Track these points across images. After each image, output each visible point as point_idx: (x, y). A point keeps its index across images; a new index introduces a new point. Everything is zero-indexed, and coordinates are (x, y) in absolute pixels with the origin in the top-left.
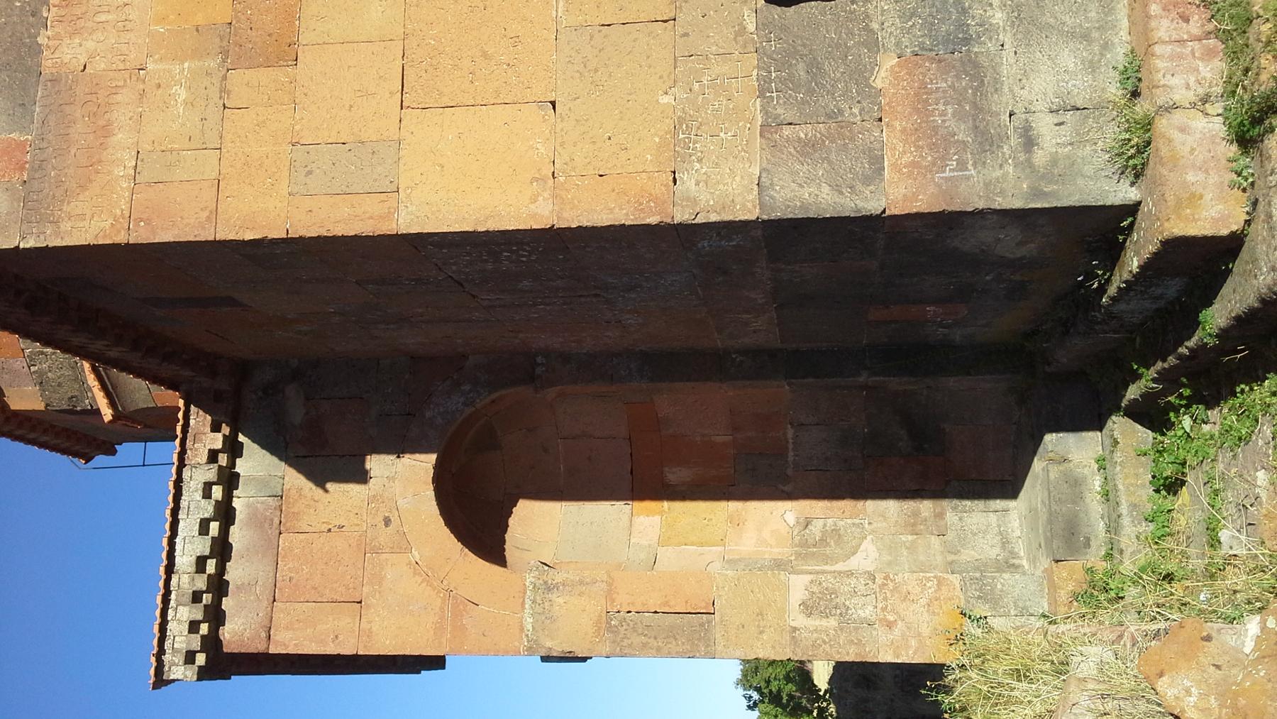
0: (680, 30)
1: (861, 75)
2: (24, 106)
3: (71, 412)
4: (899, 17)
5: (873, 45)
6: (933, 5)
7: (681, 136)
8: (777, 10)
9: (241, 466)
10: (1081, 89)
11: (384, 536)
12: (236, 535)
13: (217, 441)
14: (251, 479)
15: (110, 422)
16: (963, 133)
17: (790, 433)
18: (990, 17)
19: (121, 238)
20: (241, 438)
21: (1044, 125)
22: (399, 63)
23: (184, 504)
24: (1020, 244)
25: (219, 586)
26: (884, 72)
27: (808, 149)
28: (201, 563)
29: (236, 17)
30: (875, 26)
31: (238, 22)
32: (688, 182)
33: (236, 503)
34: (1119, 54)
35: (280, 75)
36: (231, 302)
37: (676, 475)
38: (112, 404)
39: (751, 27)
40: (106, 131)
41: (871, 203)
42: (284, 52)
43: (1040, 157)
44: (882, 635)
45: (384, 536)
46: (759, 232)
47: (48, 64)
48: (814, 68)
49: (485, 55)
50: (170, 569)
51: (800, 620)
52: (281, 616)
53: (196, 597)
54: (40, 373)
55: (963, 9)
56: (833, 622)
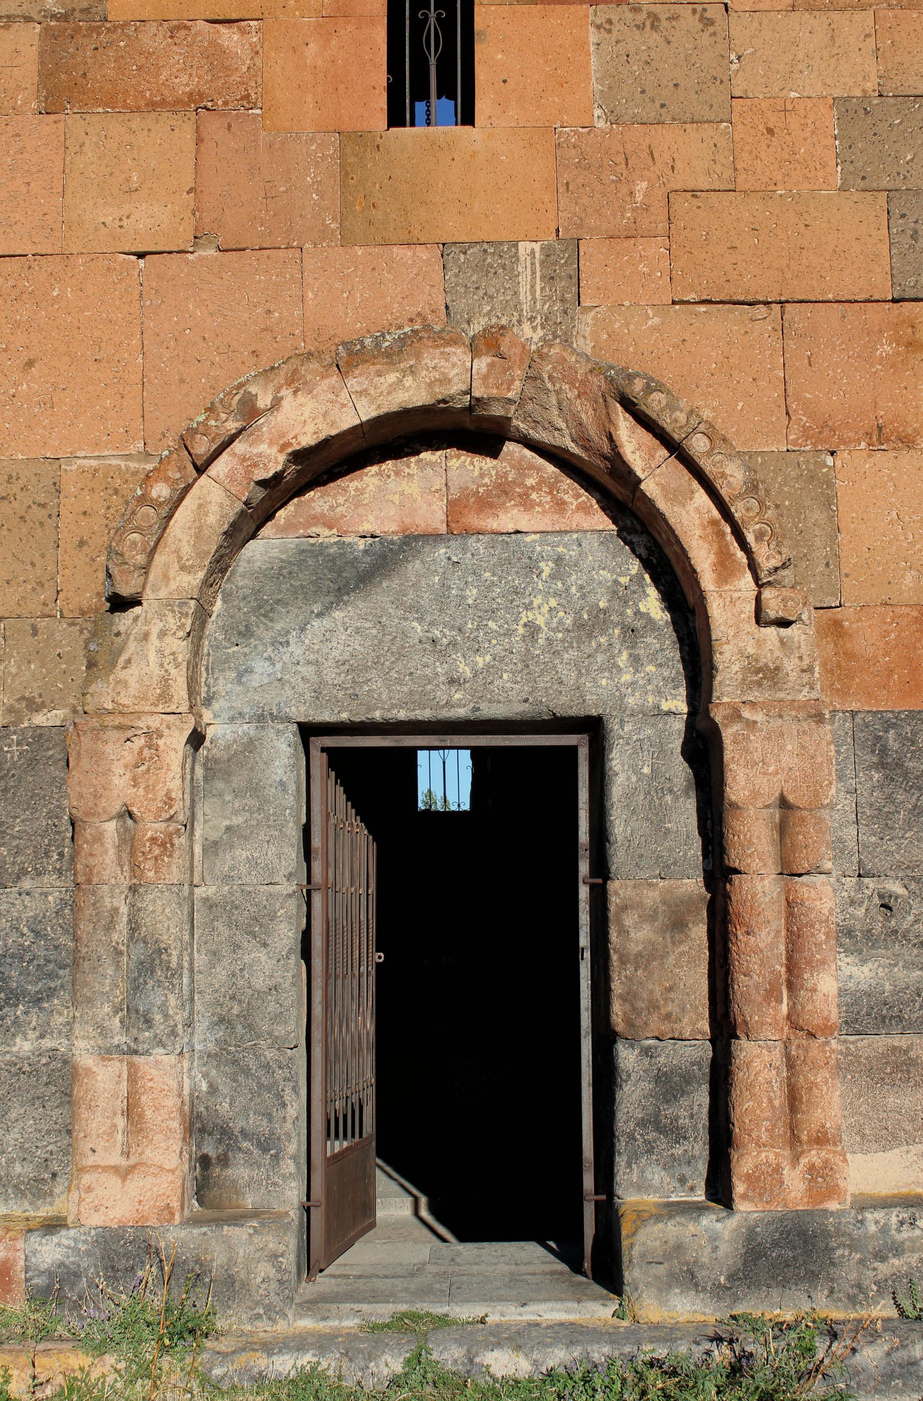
0: (42, 624)
4: (35, 917)
6: (49, 961)
18: (25, 1035)
22: (29, 249)
29: (115, 27)
30: (27, 884)
31: (108, 30)
39: (40, 719)
49: (30, 364)
55: (39, 1000)
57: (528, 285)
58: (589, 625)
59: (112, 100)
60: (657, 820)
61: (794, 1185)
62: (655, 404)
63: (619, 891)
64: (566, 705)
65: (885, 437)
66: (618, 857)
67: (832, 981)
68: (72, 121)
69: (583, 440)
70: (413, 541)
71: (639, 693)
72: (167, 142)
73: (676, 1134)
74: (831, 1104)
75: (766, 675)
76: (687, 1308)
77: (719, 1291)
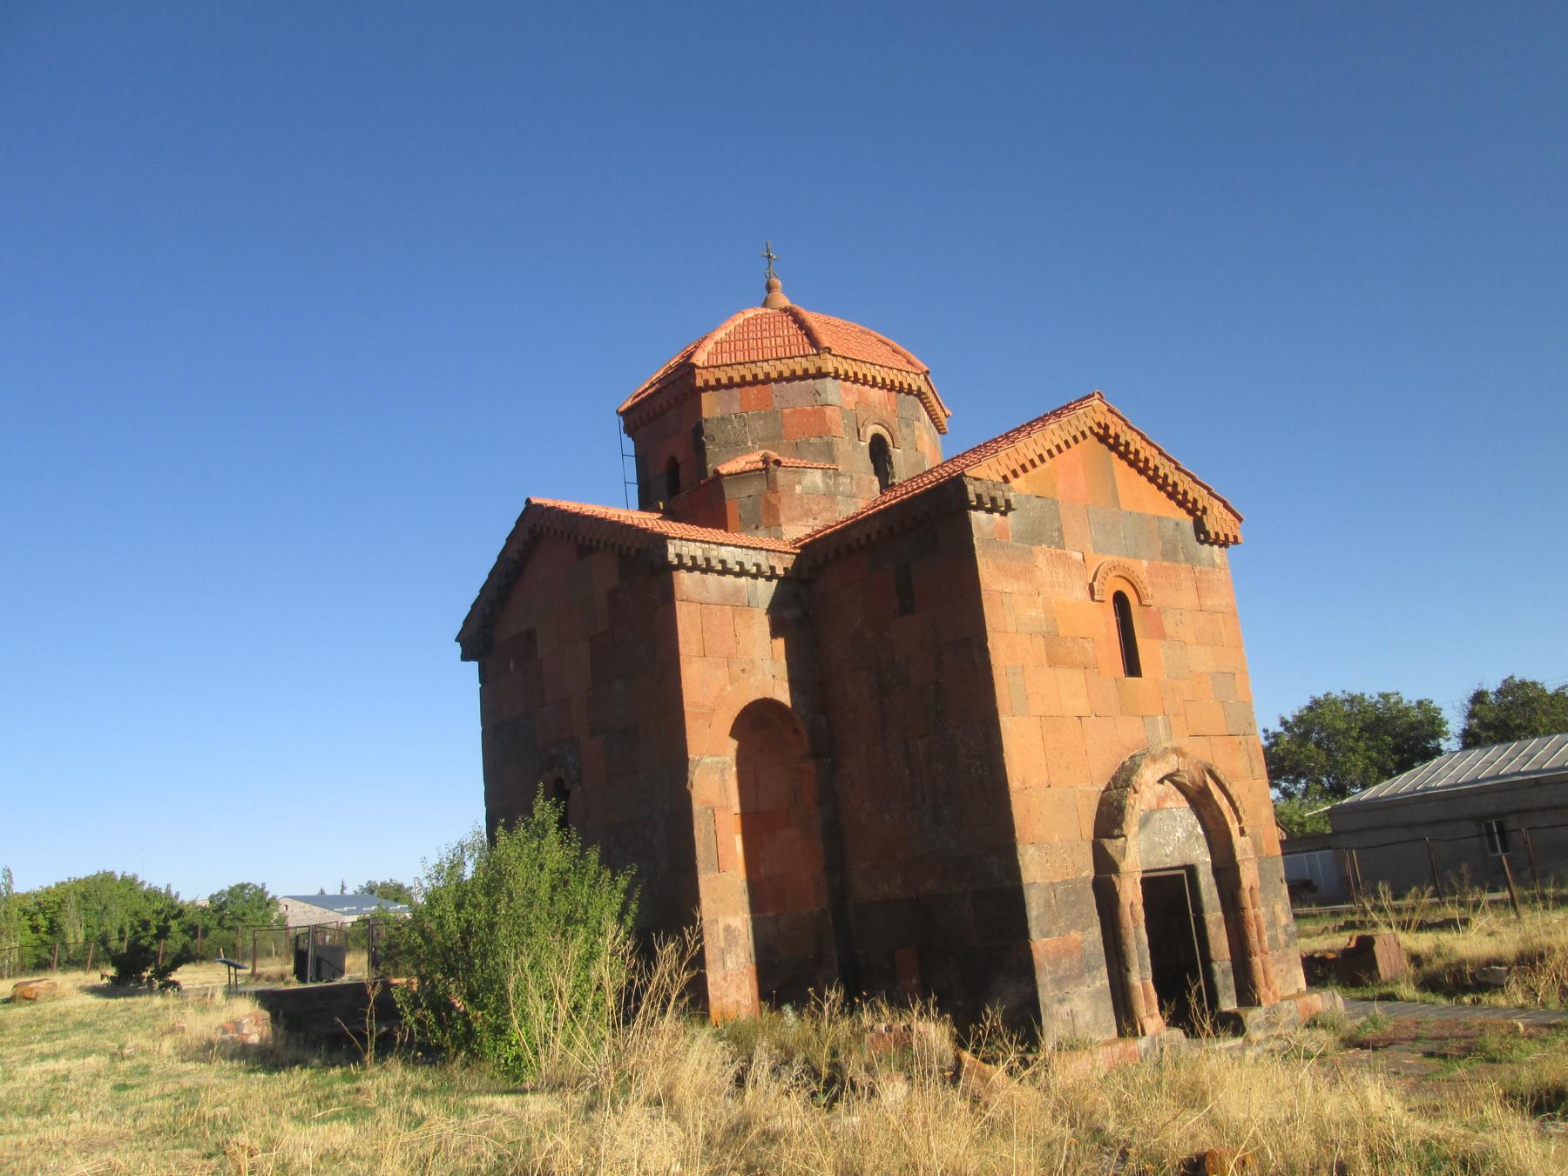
1: (1073, 925)
2: (1020, 537)
3: (698, 430)
5: (1084, 929)
9: (761, 581)
10: (1080, 1022)
11: (736, 669)
12: (729, 579)
13: (780, 572)
14: (755, 587)
15: (716, 472)
16: (1060, 972)
17: (771, 914)
19: (983, 587)
20: (775, 582)
21: (1066, 1008)
23: (751, 552)
25: (708, 569)
26: (1075, 935)
27: (1048, 903)
28: (723, 562)
33: (744, 579)
35: (1044, 660)
38: (730, 475)
39: (1084, 874)
40: (1017, 579)
41: (1034, 934)
42: (1053, 661)
43: (1056, 1006)
44: (719, 975)
45: (736, 669)
47: (1036, 549)
51: (721, 925)
52: (695, 607)
53: (708, 560)
57: (1161, 730)
58: (1188, 838)
60: (1210, 893)
62: (1218, 773)
67: (1265, 938)
69: (1193, 782)
70: (1152, 811)
71: (1202, 857)
72: (1078, 676)
73: (1228, 988)
74: (1273, 971)
75: (1245, 851)
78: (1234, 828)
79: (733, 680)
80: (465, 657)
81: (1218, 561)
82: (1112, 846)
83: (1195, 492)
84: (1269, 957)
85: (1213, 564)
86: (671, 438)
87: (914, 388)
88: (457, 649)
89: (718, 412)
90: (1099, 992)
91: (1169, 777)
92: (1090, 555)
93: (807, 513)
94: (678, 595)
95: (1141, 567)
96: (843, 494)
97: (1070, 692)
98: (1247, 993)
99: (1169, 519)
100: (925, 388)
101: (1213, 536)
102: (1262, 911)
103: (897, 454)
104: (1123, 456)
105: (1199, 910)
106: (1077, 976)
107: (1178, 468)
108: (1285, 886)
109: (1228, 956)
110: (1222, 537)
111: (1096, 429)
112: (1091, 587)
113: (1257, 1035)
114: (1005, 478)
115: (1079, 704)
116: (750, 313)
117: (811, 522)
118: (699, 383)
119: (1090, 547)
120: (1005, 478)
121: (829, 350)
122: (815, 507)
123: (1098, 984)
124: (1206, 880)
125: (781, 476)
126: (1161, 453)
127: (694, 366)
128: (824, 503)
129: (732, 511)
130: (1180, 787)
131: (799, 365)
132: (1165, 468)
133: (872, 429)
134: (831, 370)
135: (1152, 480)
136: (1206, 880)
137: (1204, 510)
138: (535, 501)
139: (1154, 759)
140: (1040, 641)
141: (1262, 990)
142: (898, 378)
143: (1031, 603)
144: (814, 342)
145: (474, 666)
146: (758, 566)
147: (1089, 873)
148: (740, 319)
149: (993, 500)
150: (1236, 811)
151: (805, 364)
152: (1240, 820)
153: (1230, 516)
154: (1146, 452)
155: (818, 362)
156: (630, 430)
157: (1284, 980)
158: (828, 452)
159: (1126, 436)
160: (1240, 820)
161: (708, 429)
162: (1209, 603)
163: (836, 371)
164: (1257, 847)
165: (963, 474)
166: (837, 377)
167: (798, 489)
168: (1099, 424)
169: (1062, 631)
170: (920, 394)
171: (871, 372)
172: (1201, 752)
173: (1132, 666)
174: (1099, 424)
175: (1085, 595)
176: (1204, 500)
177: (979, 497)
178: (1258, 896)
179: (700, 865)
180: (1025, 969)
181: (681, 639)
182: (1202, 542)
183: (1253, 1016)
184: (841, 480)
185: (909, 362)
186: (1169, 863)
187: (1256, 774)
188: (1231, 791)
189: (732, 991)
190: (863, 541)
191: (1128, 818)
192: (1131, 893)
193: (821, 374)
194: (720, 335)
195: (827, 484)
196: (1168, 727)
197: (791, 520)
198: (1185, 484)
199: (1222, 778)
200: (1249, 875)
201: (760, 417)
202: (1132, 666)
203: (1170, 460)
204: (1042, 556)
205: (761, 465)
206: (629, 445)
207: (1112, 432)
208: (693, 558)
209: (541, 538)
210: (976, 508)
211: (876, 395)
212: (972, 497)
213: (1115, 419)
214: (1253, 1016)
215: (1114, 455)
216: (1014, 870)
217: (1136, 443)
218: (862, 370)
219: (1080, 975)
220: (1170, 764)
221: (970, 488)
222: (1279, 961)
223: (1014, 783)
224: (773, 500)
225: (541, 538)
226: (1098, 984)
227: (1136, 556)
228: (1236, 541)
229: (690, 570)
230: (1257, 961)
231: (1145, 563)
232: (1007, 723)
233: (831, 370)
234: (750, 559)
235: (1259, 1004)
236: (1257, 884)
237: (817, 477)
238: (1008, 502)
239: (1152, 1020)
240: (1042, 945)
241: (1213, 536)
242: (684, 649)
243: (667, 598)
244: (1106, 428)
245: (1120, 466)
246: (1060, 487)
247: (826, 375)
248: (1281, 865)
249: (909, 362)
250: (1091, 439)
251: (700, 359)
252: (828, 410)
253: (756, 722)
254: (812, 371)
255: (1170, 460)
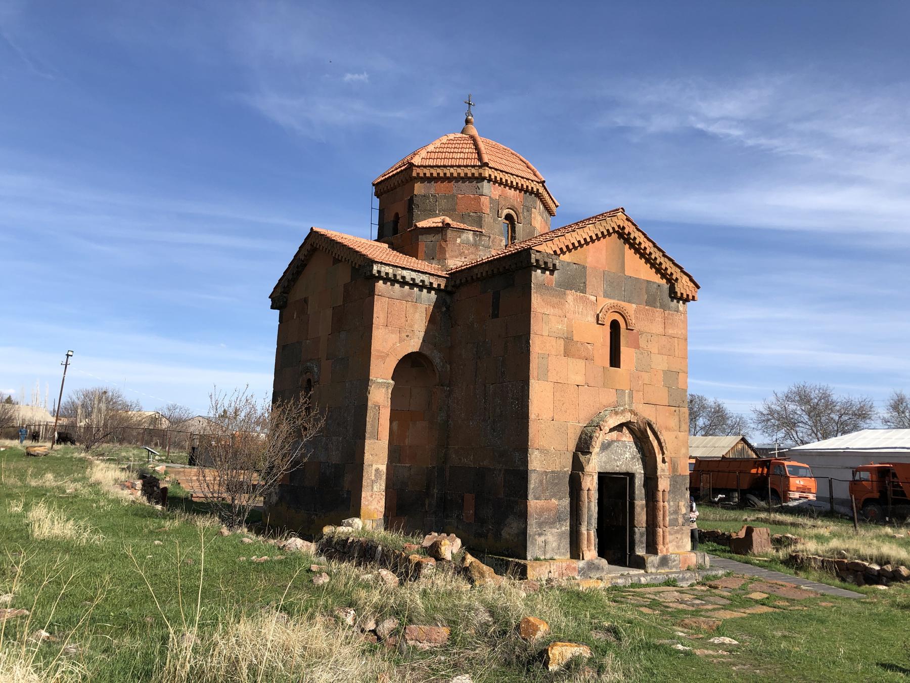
3: (411, 201)
5: (560, 499)
7: (544, 451)
8: (568, 476)
21: (543, 538)
24: (509, 534)
26: (554, 501)
27: (541, 482)
28: (403, 278)
32: (536, 453)
34: (555, 557)
35: (562, 352)
36: (495, 315)
37: (395, 424)
38: (423, 228)
40: (554, 307)
41: (530, 497)
42: (567, 354)
44: (369, 494)
45: (404, 335)
46: (522, 468)
47: (568, 292)
48: (557, 484)
50: (403, 268)
53: (395, 276)
54: (429, 198)
56: (373, 478)
57: (627, 399)
58: (633, 458)
59: (573, 356)
61: (665, 553)
62: (654, 426)
63: (636, 502)
64: (630, 471)
65: (668, 429)
66: (636, 497)
67: (667, 519)
68: (570, 360)
71: (638, 469)
72: (581, 363)
73: (642, 543)
74: (669, 538)
75: (663, 470)
76: (654, 570)
77: (657, 568)
78: (659, 458)
79: (401, 340)
80: (272, 308)
81: (681, 308)
82: (582, 458)
83: (672, 269)
84: (667, 530)
85: (677, 311)
86: (399, 204)
87: (535, 190)
88: (270, 302)
89: (423, 192)
90: (563, 533)
91: (627, 425)
92: (601, 299)
93: (461, 254)
94: (376, 293)
95: (631, 308)
96: (483, 246)
97: (575, 371)
98: (652, 548)
99: (654, 283)
100: (541, 190)
101: (679, 295)
102: (666, 503)
103: (519, 227)
104: (632, 246)
105: (632, 498)
106: (552, 523)
107: (664, 256)
108: (688, 492)
109: (644, 525)
110: (685, 296)
111: (617, 229)
112: (598, 315)
113: (651, 570)
114: (555, 252)
115: (580, 379)
116: (451, 136)
117: (463, 259)
118: (414, 174)
119: (601, 294)
120: (555, 252)
121: (486, 165)
122: (466, 252)
123: (563, 529)
124: (639, 481)
125: (449, 233)
126: (655, 246)
127: (411, 165)
128: (472, 249)
129: (422, 248)
130: (632, 431)
131: (469, 172)
132: (656, 254)
133: (506, 212)
134: (487, 175)
135: (648, 261)
136: (639, 481)
137: (677, 279)
138: (315, 229)
139: (616, 413)
140: (562, 342)
141: (660, 547)
142: (526, 183)
143: (561, 324)
144: (480, 158)
145: (277, 312)
146: (423, 281)
147: (568, 469)
148: (444, 139)
149: (546, 263)
150: (661, 448)
151: (473, 170)
152: (663, 453)
153: (692, 285)
154: (646, 244)
155: (481, 171)
156: (378, 195)
157: (678, 542)
158: (479, 221)
159: (635, 234)
160: (663, 453)
161: (415, 200)
162: (670, 332)
163: (490, 175)
164: (674, 468)
165: (531, 248)
166: (490, 180)
167: (459, 240)
168: (619, 226)
169: (575, 339)
170: (538, 195)
171: (510, 179)
172: (648, 413)
173: (615, 360)
174: (619, 226)
175: (594, 320)
176: (677, 274)
177: (537, 261)
178: (667, 497)
179: (367, 435)
180: (523, 515)
181: (375, 315)
182: (672, 298)
183: (652, 560)
184: (483, 238)
185: (535, 175)
186: (617, 470)
187: (682, 429)
188: (661, 437)
189: (375, 503)
190: (479, 276)
191: (593, 443)
192: (590, 483)
193: (481, 179)
194: (431, 148)
195: (475, 239)
196: (631, 397)
197: (452, 257)
198: (666, 264)
199: (656, 429)
200: (663, 484)
201: (445, 197)
202: (615, 360)
203: (659, 250)
204: (571, 296)
205: (440, 225)
206: (376, 202)
207: (626, 231)
208: (387, 274)
209: (316, 248)
210: (538, 267)
211: (512, 193)
212: (533, 261)
213: (630, 224)
214: (652, 560)
215: (627, 246)
216: (525, 462)
217: (640, 239)
218: (505, 177)
219: (554, 523)
220: (627, 417)
221: (533, 256)
222: (677, 532)
223: (532, 416)
224: (443, 244)
225: (316, 248)
226: (563, 529)
227: (629, 302)
228: (693, 297)
229: (386, 279)
230: (660, 531)
231: (634, 306)
232: (532, 382)
233: (487, 175)
234: (418, 278)
235: (655, 552)
236: (667, 490)
237: (470, 236)
238: (554, 265)
239: (590, 553)
240: (534, 504)
241: (679, 295)
242: (375, 321)
243: (371, 293)
244: (624, 228)
245: (629, 253)
246: (589, 260)
247: (485, 178)
248: (688, 481)
249: (535, 175)
250: (615, 236)
251: (417, 161)
252: (483, 198)
253: (409, 366)
254: (476, 175)
255: (659, 250)
